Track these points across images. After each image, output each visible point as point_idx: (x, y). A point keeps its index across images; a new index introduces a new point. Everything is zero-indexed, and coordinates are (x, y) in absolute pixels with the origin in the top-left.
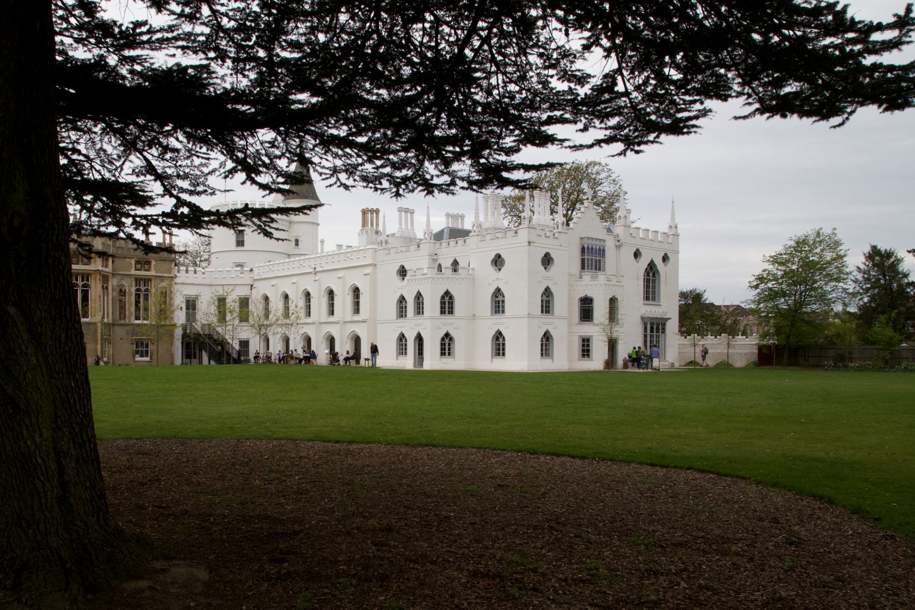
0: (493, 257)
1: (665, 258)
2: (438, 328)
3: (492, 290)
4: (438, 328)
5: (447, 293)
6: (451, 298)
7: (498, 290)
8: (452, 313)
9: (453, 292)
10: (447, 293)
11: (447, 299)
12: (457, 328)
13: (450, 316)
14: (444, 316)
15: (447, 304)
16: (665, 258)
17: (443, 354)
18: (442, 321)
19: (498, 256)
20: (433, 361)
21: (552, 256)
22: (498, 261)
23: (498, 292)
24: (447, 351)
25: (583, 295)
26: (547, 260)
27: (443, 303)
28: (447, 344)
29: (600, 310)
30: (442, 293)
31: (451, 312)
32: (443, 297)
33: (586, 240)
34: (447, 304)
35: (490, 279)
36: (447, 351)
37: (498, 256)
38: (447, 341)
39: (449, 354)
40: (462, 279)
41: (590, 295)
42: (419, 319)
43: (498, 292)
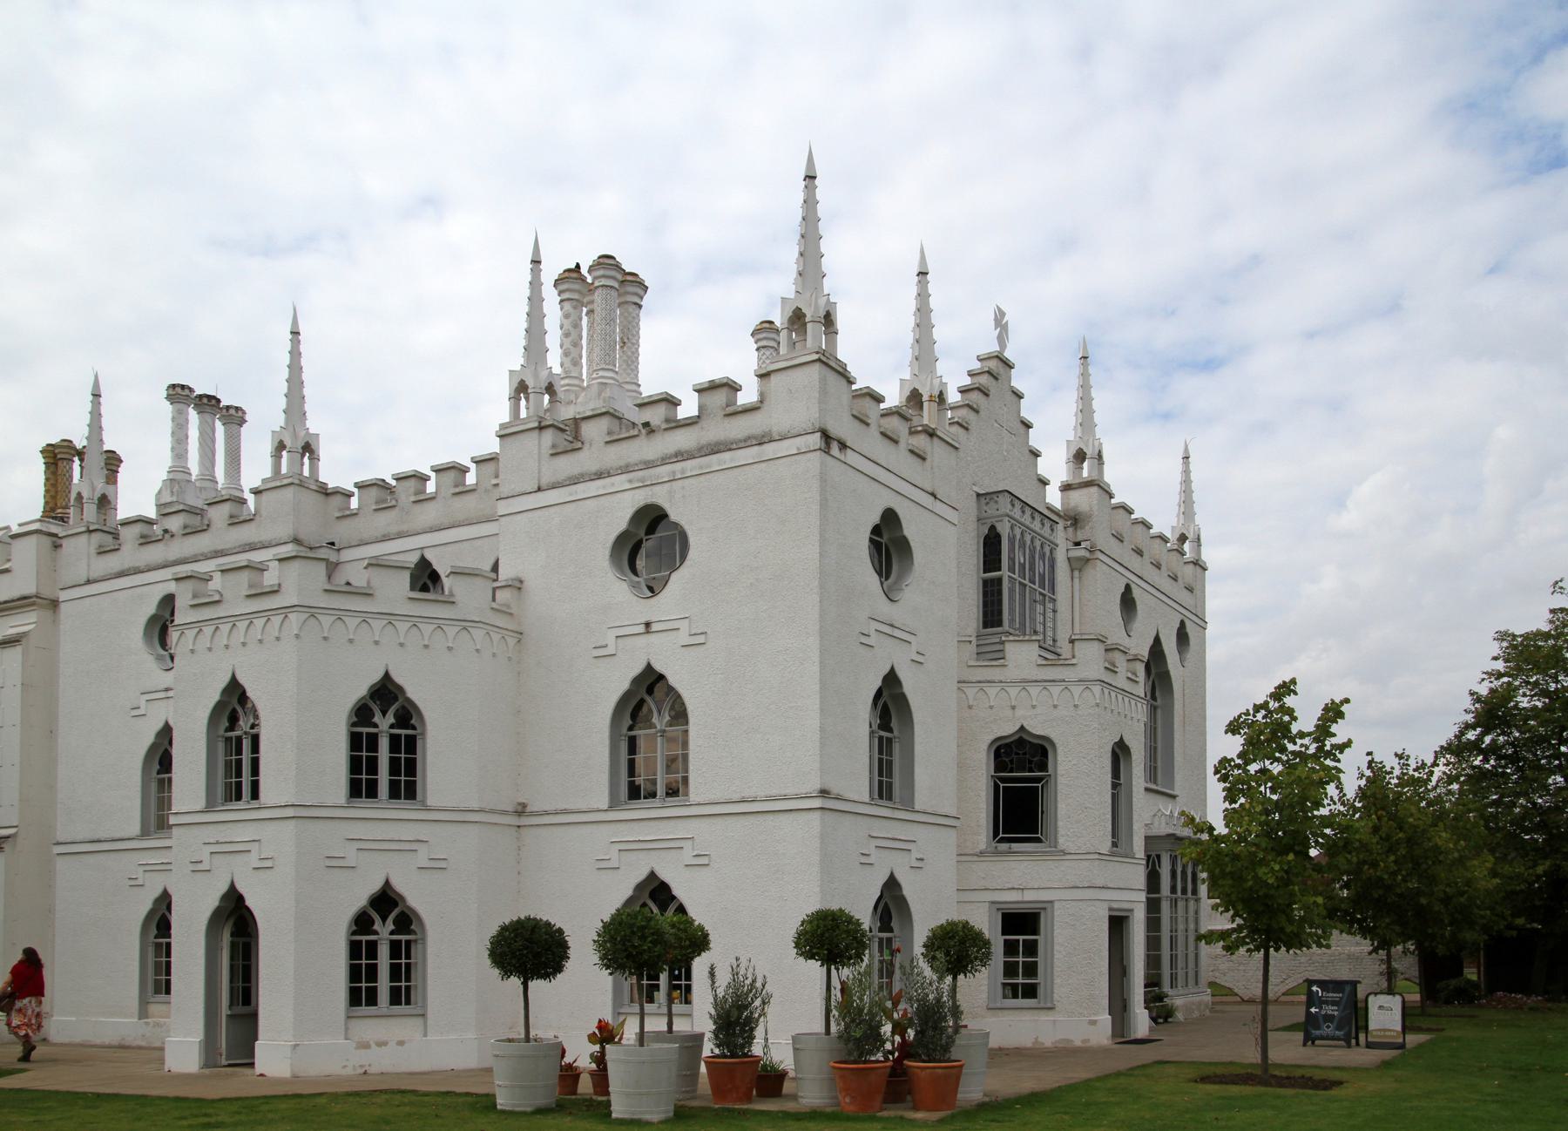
0: (621, 522)
1: (1182, 637)
2: (336, 864)
3: (619, 681)
4: (336, 864)
5: (385, 692)
6: (408, 716)
7: (651, 682)
8: (411, 793)
9: (415, 690)
10: (385, 692)
11: (384, 723)
12: (436, 867)
13: (402, 810)
14: (364, 808)
15: (384, 748)
16: (1182, 637)
17: (360, 995)
18: (359, 830)
19: (652, 519)
20: (306, 1033)
21: (909, 530)
22: (649, 543)
23: (649, 698)
24: (384, 984)
25: (1008, 729)
26: (889, 546)
27: (361, 745)
28: (383, 952)
29: (1077, 792)
30: (361, 690)
31: (406, 787)
32: (362, 714)
33: (1004, 504)
34: (384, 748)
35: (599, 629)
36: (384, 984)
37: (652, 519)
38: (384, 931)
39: (396, 998)
40: (466, 625)
41: (1037, 728)
42: (238, 824)
43: (649, 698)
